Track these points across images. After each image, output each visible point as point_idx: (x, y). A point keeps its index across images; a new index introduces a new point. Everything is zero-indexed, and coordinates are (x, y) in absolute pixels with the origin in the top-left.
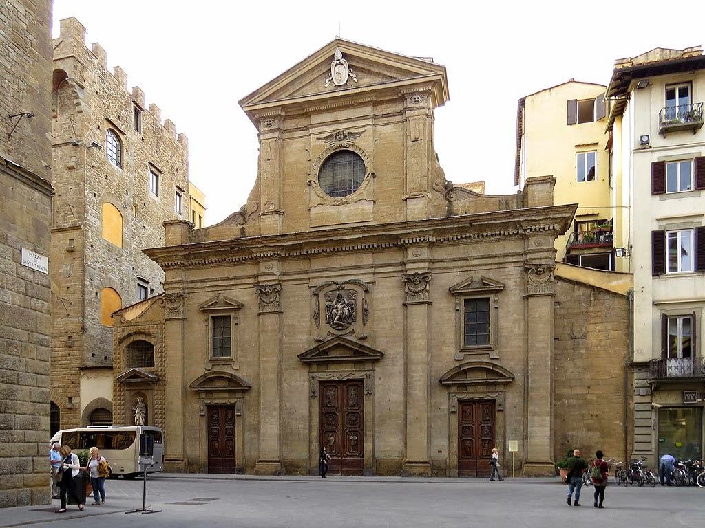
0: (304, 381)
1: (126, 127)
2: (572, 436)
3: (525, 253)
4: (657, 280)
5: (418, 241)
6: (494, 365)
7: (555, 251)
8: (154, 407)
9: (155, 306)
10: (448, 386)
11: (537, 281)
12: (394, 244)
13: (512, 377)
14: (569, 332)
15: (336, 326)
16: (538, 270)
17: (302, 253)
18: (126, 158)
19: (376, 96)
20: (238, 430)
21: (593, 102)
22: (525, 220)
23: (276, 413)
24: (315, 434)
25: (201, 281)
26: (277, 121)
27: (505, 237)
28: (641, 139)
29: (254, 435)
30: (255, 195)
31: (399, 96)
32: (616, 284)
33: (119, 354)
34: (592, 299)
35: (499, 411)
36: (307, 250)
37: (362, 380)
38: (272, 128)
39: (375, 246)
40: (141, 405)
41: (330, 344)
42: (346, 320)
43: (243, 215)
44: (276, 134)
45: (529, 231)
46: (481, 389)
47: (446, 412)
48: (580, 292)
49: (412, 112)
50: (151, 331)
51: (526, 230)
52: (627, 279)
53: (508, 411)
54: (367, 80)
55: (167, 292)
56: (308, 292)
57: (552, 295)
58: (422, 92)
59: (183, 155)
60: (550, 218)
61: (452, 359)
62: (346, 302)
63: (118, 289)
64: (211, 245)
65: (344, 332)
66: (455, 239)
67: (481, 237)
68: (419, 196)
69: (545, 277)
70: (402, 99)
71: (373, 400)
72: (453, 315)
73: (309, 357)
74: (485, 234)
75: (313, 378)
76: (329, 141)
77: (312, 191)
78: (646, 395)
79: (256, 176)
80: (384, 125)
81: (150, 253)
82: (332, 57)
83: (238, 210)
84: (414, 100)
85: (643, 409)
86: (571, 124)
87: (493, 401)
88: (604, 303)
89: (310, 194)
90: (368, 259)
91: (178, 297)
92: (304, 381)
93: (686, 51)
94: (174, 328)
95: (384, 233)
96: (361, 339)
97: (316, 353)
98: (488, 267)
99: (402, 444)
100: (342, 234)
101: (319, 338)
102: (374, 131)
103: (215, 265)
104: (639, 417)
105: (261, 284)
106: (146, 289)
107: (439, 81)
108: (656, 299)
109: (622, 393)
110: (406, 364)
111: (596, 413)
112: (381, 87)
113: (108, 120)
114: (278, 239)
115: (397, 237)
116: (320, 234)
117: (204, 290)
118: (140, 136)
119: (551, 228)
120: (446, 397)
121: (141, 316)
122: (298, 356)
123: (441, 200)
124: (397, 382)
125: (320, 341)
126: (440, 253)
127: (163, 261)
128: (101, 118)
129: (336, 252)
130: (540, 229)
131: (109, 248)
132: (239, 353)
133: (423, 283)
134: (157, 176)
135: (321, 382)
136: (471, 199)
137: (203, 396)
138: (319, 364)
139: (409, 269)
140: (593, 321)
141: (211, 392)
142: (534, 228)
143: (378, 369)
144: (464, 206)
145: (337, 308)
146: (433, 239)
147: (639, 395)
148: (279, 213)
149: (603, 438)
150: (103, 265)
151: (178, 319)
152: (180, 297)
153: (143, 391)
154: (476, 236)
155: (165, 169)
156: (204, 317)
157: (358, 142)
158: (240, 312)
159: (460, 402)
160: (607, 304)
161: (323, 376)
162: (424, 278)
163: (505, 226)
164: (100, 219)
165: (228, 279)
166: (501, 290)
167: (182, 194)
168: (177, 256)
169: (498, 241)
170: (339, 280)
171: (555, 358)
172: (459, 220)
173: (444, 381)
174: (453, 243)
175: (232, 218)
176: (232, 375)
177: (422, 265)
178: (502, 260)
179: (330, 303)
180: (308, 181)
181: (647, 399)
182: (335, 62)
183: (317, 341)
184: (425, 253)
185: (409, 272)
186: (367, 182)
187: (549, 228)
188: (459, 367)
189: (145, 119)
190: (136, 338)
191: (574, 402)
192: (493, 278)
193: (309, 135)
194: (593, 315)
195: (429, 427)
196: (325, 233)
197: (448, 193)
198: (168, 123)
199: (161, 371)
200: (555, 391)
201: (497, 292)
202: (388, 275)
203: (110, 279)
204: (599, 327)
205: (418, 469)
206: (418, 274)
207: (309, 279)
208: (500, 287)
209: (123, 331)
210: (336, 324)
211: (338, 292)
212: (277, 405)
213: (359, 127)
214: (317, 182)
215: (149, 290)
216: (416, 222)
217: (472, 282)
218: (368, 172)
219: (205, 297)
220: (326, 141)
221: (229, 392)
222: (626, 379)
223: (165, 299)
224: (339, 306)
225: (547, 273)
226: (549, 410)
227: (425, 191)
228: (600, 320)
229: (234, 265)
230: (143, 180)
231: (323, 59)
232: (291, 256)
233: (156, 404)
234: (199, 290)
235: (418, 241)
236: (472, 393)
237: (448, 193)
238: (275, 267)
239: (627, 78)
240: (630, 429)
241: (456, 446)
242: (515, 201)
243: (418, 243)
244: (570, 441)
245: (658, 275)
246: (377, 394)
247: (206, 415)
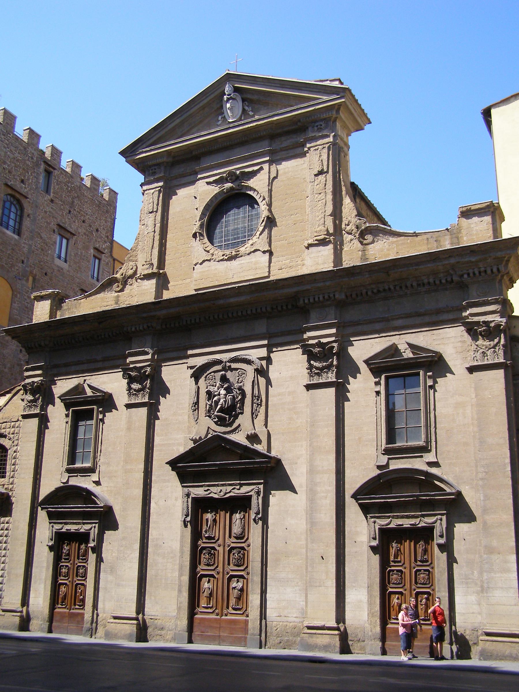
5: (321, 299)
12: (293, 306)
45: (465, 276)
51: (462, 276)
67: (404, 288)
130: (480, 272)
142: (471, 271)
144: (382, 250)
154: (398, 288)
161: (199, 492)
187: (492, 270)
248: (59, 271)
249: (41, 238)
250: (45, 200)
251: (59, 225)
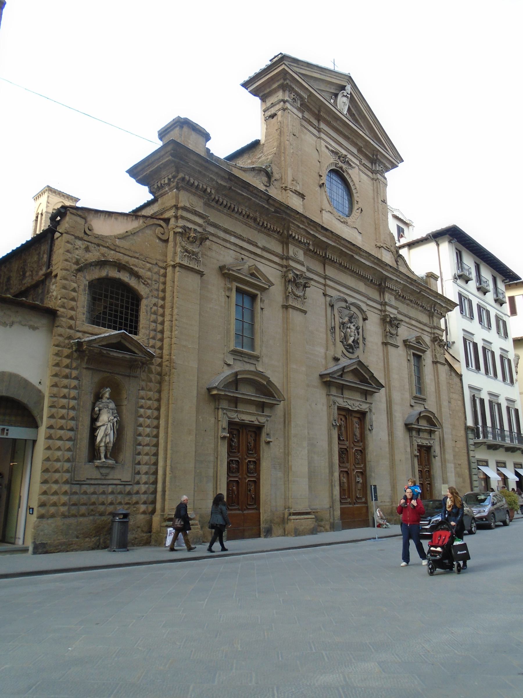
100: (360, 255)
116: (349, 245)
170: (350, 300)
196: (352, 247)
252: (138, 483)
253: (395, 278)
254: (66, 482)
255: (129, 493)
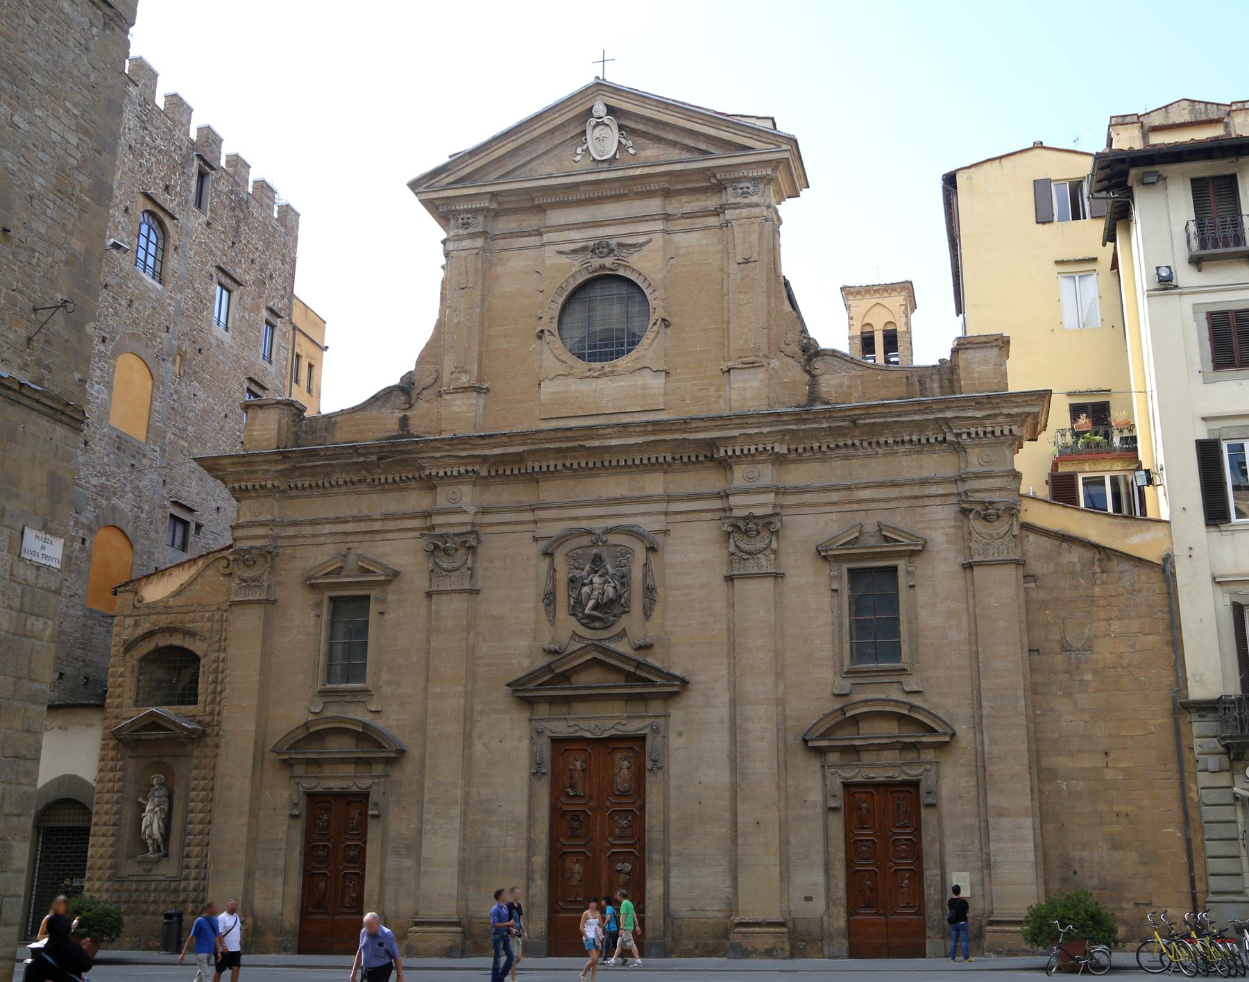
0: (520, 739)
1: (179, 204)
2: (1081, 861)
3: (962, 479)
4: (1215, 535)
5: (753, 451)
6: (912, 707)
7: (1017, 476)
8: (188, 795)
9: (210, 572)
10: (820, 752)
11: (988, 534)
12: (706, 456)
13: (950, 732)
14: (1058, 638)
15: (587, 622)
16: (988, 512)
17: (523, 471)
18: (173, 262)
19: (668, 182)
20: (372, 849)
21: (1081, 182)
22: (956, 417)
23: (456, 812)
24: (540, 860)
25: (313, 523)
26: (481, 218)
27: (920, 447)
28: (1158, 274)
29: (408, 863)
30: (430, 355)
31: (716, 184)
32: (1138, 542)
33: (121, 675)
34: (1097, 569)
35: (928, 806)
36: (532, 464)
37: (642, 739)
38: (471, 230)
39: (669, 459)
40: (159, 793)
41: (576, 658)
42: (610, 609)
43: (406, 389)
44: (479, 242)
45: (965, 436)
46: (889, 756)
47: (819, 810)
48: (1074, 556)
49: (738, 211)
50: (197, 626)
51: (960, 435)
52: (1157, 532)
53: (945, 807)
54: (652, 152)
55: (239, 545)
56: (535, 550)
57: (1020, 563)
58: (754, 179)
59: (285, 245)
60: (1001, 414)
61: (827, 694)
62: (611, 571)
63: (129, 529)
64: (335, 454)
65: (605, 634)
66: (824, 448)
67: (874, 445)
68: (753, 365)
69: (1002, 527)
70: (720, 187)
71: (666, 781)
72: (826, 599)
73: (531, 686)
74: (882, 440)
75: (540, 733)
76: (581, 257)
77: (546, 349)
78: (1221, 771)
79: (437, 317)
80: (685, 231)
81: (211, 466)
82: (589, 113)
83: (396, 381)
84: (740, 191)
85: (1217, 802)
86: (1044, 223)
87: (914, 785)
88: (1120, 578)
89: (541, 354)
90: (654, 484)
91: (264, 556)
92: (520, 739)
93: (1234, 107)
94: (248, 622)
95: (686, 436)
96: (640, 648)
97: (546, 678)
98: (891, 505)
99: (728, 882)
100: (602, 437)
101: (553, 647)
102: (665, 242)
103: (344, 489)
104: (1212, 819)
105: (438, 531)
106: (186, 524)
107: (785, 161)
108: (1218, 572)
109: (1173, 766)
110: (733, 703)
111: (1123, 809)
112: (678, 167)
113: (147, 196)
114: (473, 442)
115: (712, 443)
116: (559, 435)
117: (316, 540)
118: (203, 219)
119: (1006, 432)
120: (819, 776)
121: (178, 593)
122: (508, 685)
123: (795, 373)
124: (718, 741)
125: (556, 652)
126: (796, 475)
127: (237, 481)
128: (132, 192)
129: (590, 469)
130: (985, 433)
131: (121, 443)
132: (385, 676)
133: (764, 534)
134: (229, 292)
135: (556, 742)
136: (853, 372)
137: (300, 770)
138: (553, 701)
139: (737, 506)
140: (1102, 614)
141: (318, 763)
142: (973, 431)
143: (677, 714)
144: (840, 386)
145: (591, 583)
146: (781, 449)
147: (1207, 771)
148: (478, 390)
149: (1145, 863)
150: (103, 480)
151: (258, 602)
152: (268, 555)
153: (165, 760)
154: (865, 444)
155: (247, 277)
156: (311, 598)
157: (635, 260)
158: (390, 588)
159: (847, 786)
160: (1127, 580)
161: (561, 728)
162: (767, 525)
163: (921, 426)
164: (109, 386)
165: (369, 519)
166: (920, 551)
167: (278, 322)
168: (267, 471)
169: (908, 453)
170: (597, 525)
171: (1034, 690)
172: (830, 414)
173: (812, 740)
174: (821, 456)
175: (385, 396)
176: (365, 726)
177: (762, 498)
178: (917, 491)
179: (577, 573)
180: (539, 329)
181: (1224, 780)
182: (593, 121)
183: (550, 652)
184: (767, 474)
185: (736, 513)
186: (654, 334)
187: (1002, 431)
188: (842, 710)
189: (217, 187)
190: (164, 641)
191: (1080, 785)
192: (901, 526)
193: (543, 245)
194: (1102, 603)
195: (784, 843)
196: (569, 434)
197: (809, 360)
198: (263, 187)
199: (211, 714)
200: (1038, 762)
201: (913, 554)
202: (696, 516)
203: (114, 508)
204: (1115, 627)
205: (764, 941)
206: (755, 517)
207: (536, 522)
208: (916, 545)
209: (136, 624)
210: (589, 617)
211: (595, 551)
212: (459, 793)
213: (638, 234)
214: (556, 332)
215: (193, 526)
216: (748, 416)
217: (861, 532)
218: (656, 317)
219: (319, 556)
220: (575, 256)
221: (358, 761)
222: (1178, 736)
223: (235, 560)
224: (597, 580)
225: (1005, 518)
226: (1028, 803)
227: (766, 357)
228: (1115, 613)
229: (383, 491)
230: (203, 302)
231: (571, 115)
232: (499, 476)
233: (194, 790)
234: (307, 541)
235: (753, 451)
236: (872, 766)
237: (809, 360)
238: (467, 496)
239: (1120, 167)
240: (1196, 844)
241: (842, 884)
242: (936, 377)
243: (753, 456)
244: (1079, 873)
245: (1216, 525)
246: (674, 770)
247: (304, 816)
248: (218, 346)
249: (194, 289)
250: (199, 224)
251: (219, 268)
252: (186, 879)
253: (735, 433)
254: (109, 879)
255: (176, 891)
